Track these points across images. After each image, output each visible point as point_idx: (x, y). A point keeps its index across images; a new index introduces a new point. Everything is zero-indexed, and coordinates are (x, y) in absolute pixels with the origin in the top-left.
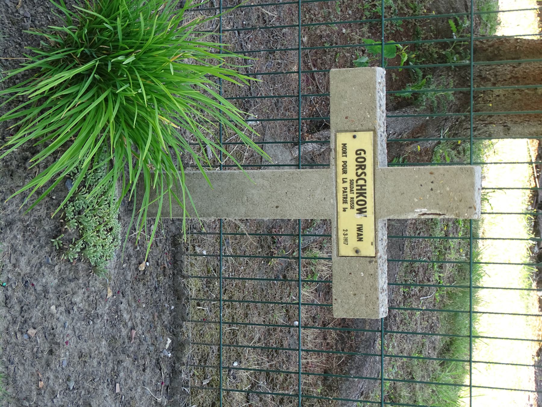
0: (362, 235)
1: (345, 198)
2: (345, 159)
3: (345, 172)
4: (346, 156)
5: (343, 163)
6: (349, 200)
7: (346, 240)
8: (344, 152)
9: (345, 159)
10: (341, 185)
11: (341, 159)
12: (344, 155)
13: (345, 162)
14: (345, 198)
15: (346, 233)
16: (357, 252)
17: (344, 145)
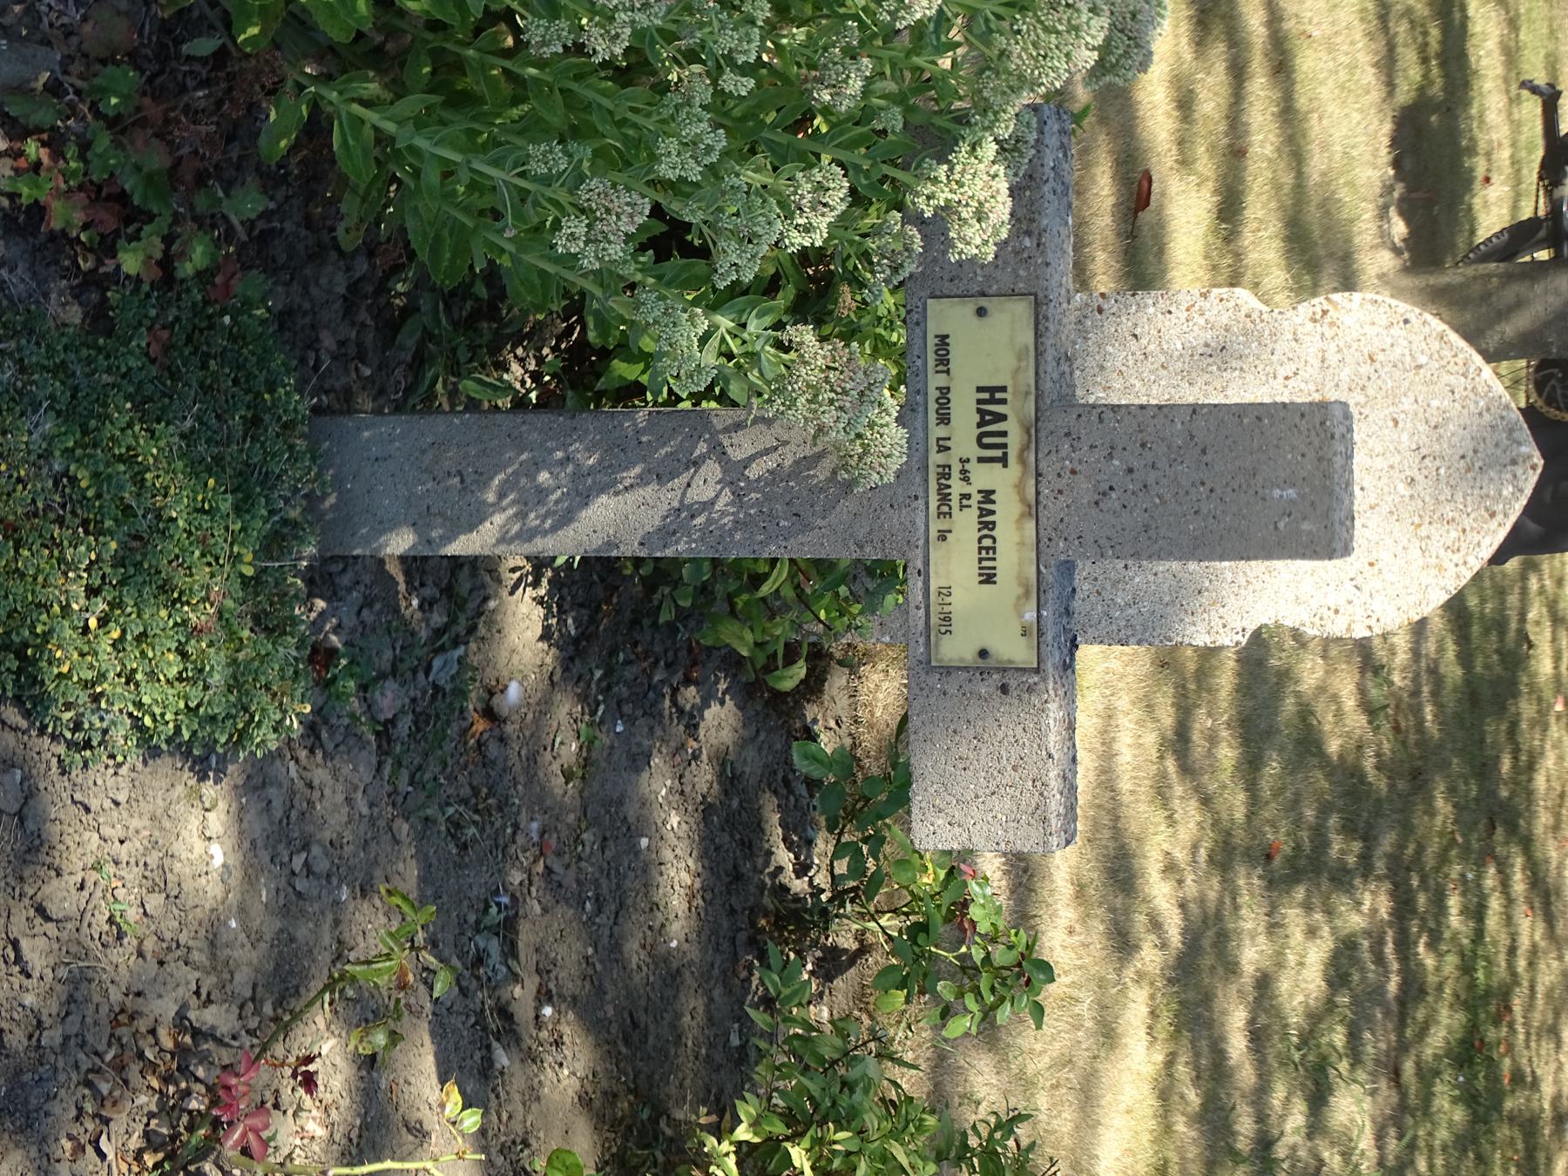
0: (993, 512)
1: (944, 498)
2: (941, 380)
3: (944, 419)
4: (948, 372)
5: (938, 394)
6: (955, 503)
7: (947, 619)
8: (943, 361)
9: (941, 380)
10: (935, 458)
11: (936, 381)
12: (940, 368)
13: (944, 391)
14: (944, 498)
15: (948, 600)
16: (983, 653)
17: (943, 339)
